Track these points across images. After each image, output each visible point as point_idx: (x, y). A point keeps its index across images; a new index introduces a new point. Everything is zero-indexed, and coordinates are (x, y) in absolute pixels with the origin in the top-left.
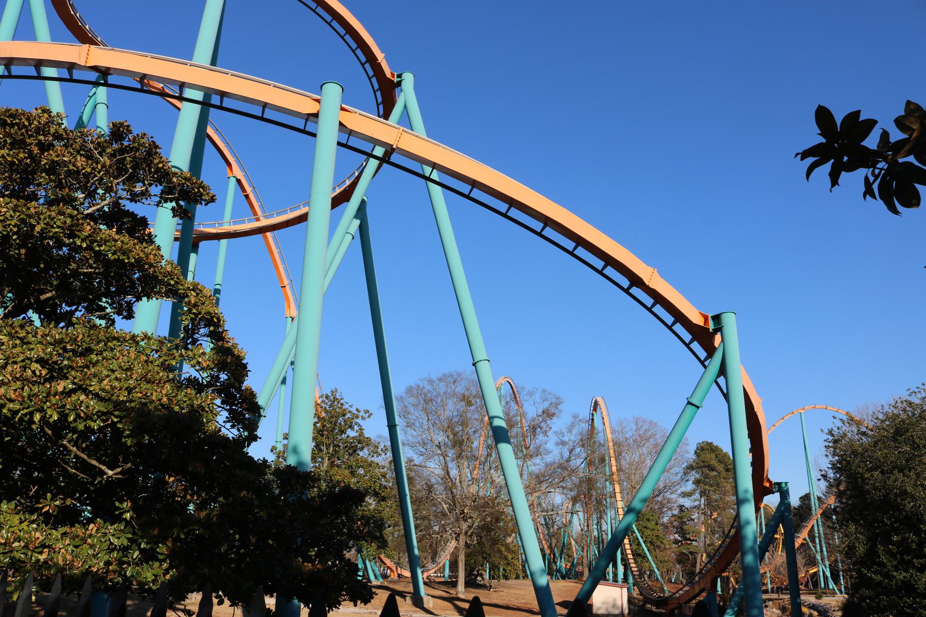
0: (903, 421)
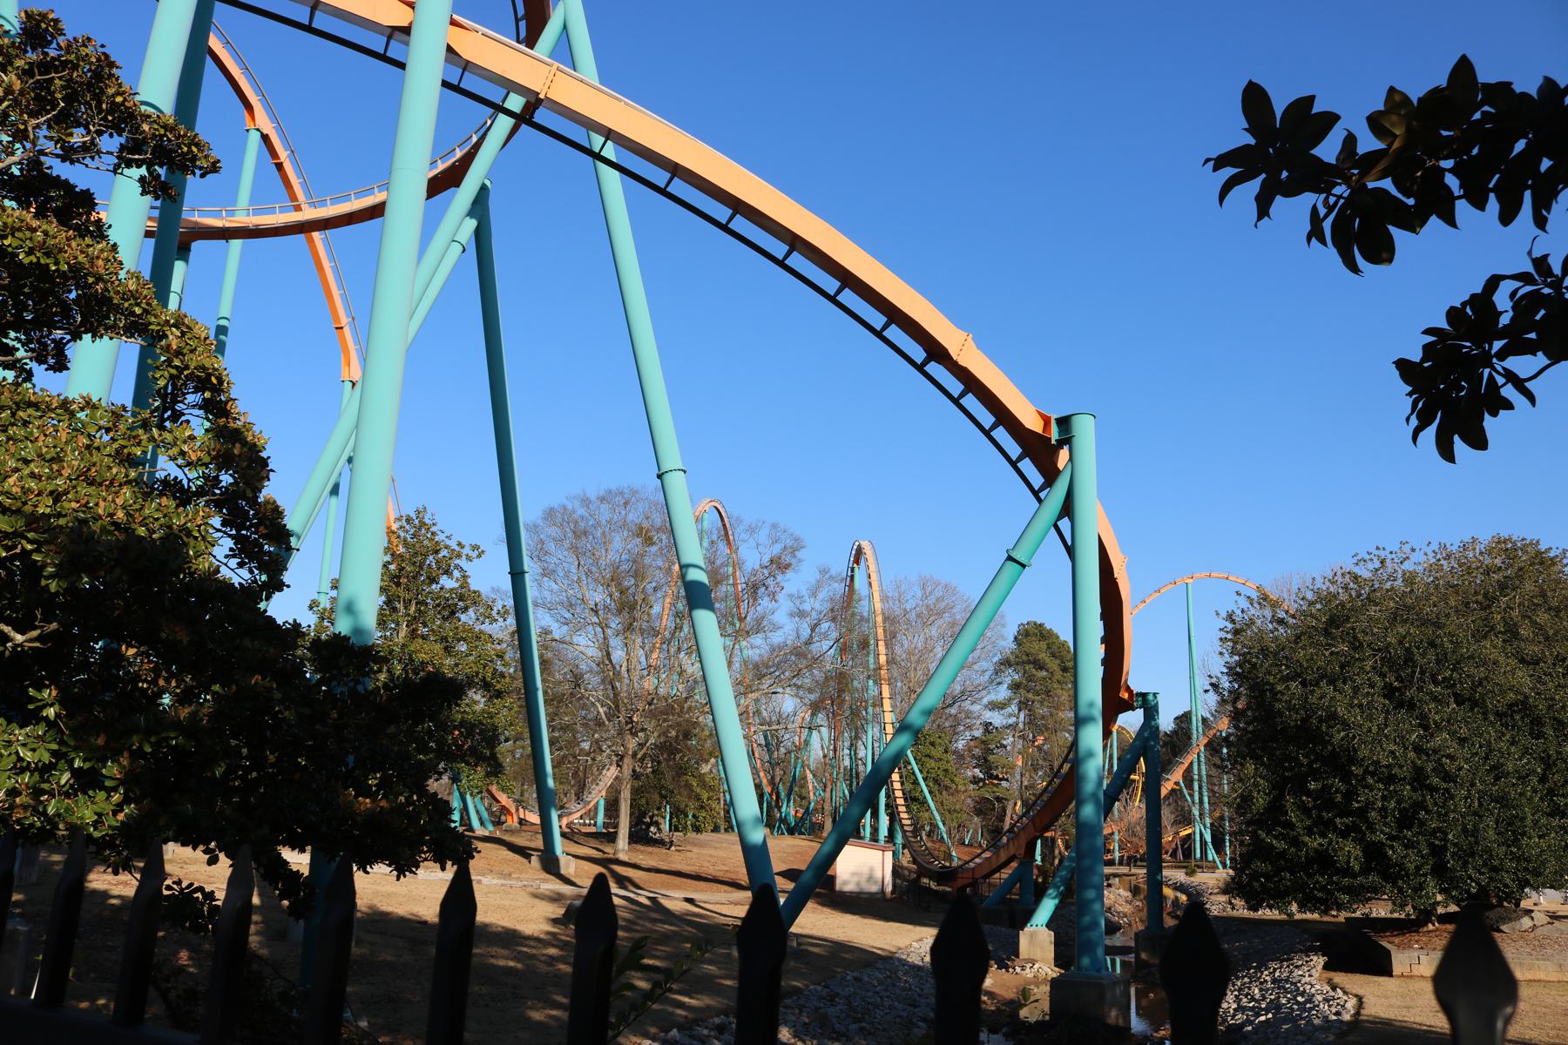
0: (1342, 604)
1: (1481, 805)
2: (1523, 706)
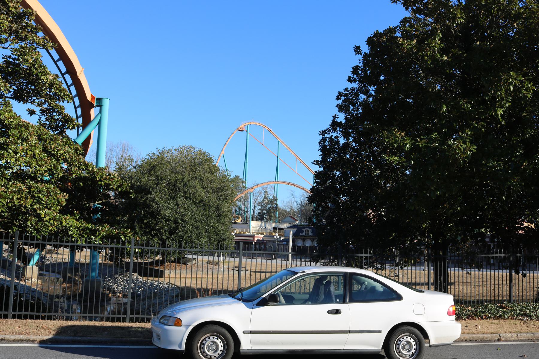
1: (192, 229)
2: (201, 201)
